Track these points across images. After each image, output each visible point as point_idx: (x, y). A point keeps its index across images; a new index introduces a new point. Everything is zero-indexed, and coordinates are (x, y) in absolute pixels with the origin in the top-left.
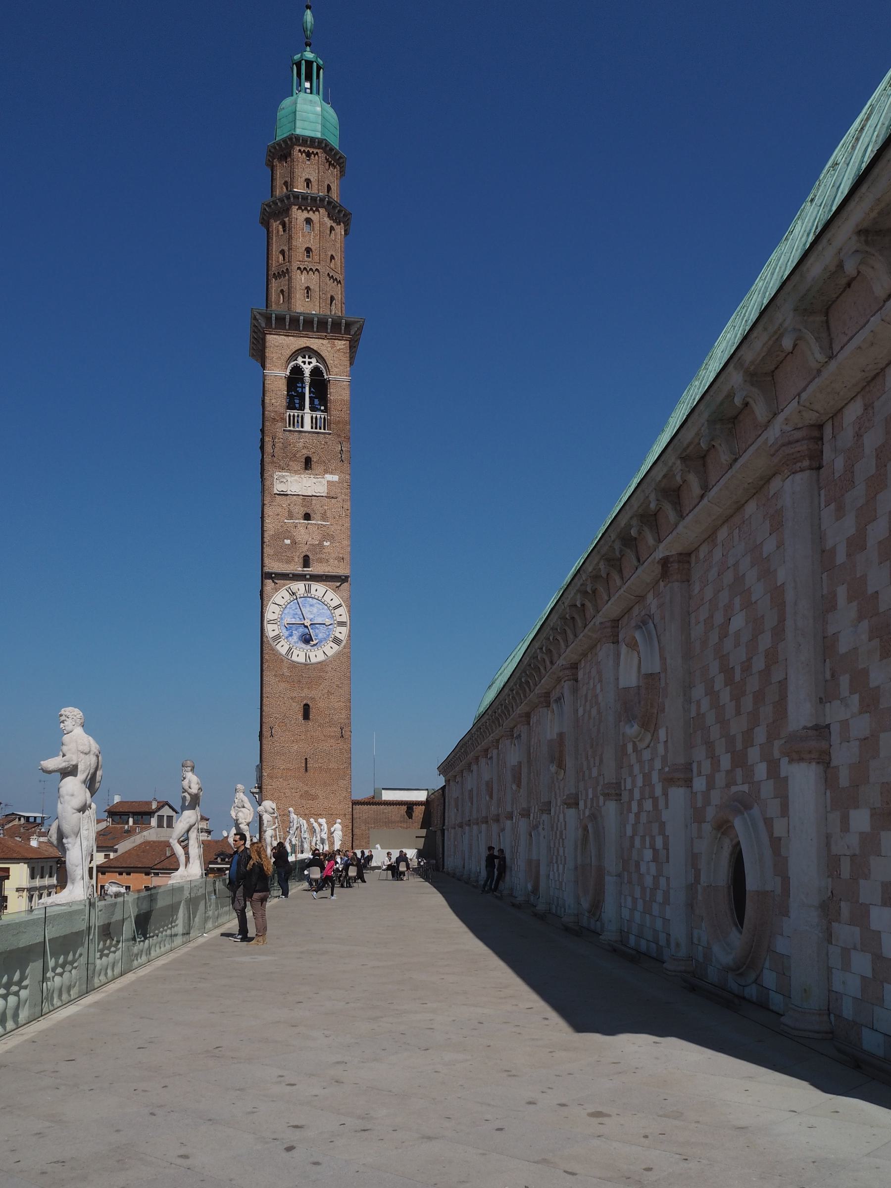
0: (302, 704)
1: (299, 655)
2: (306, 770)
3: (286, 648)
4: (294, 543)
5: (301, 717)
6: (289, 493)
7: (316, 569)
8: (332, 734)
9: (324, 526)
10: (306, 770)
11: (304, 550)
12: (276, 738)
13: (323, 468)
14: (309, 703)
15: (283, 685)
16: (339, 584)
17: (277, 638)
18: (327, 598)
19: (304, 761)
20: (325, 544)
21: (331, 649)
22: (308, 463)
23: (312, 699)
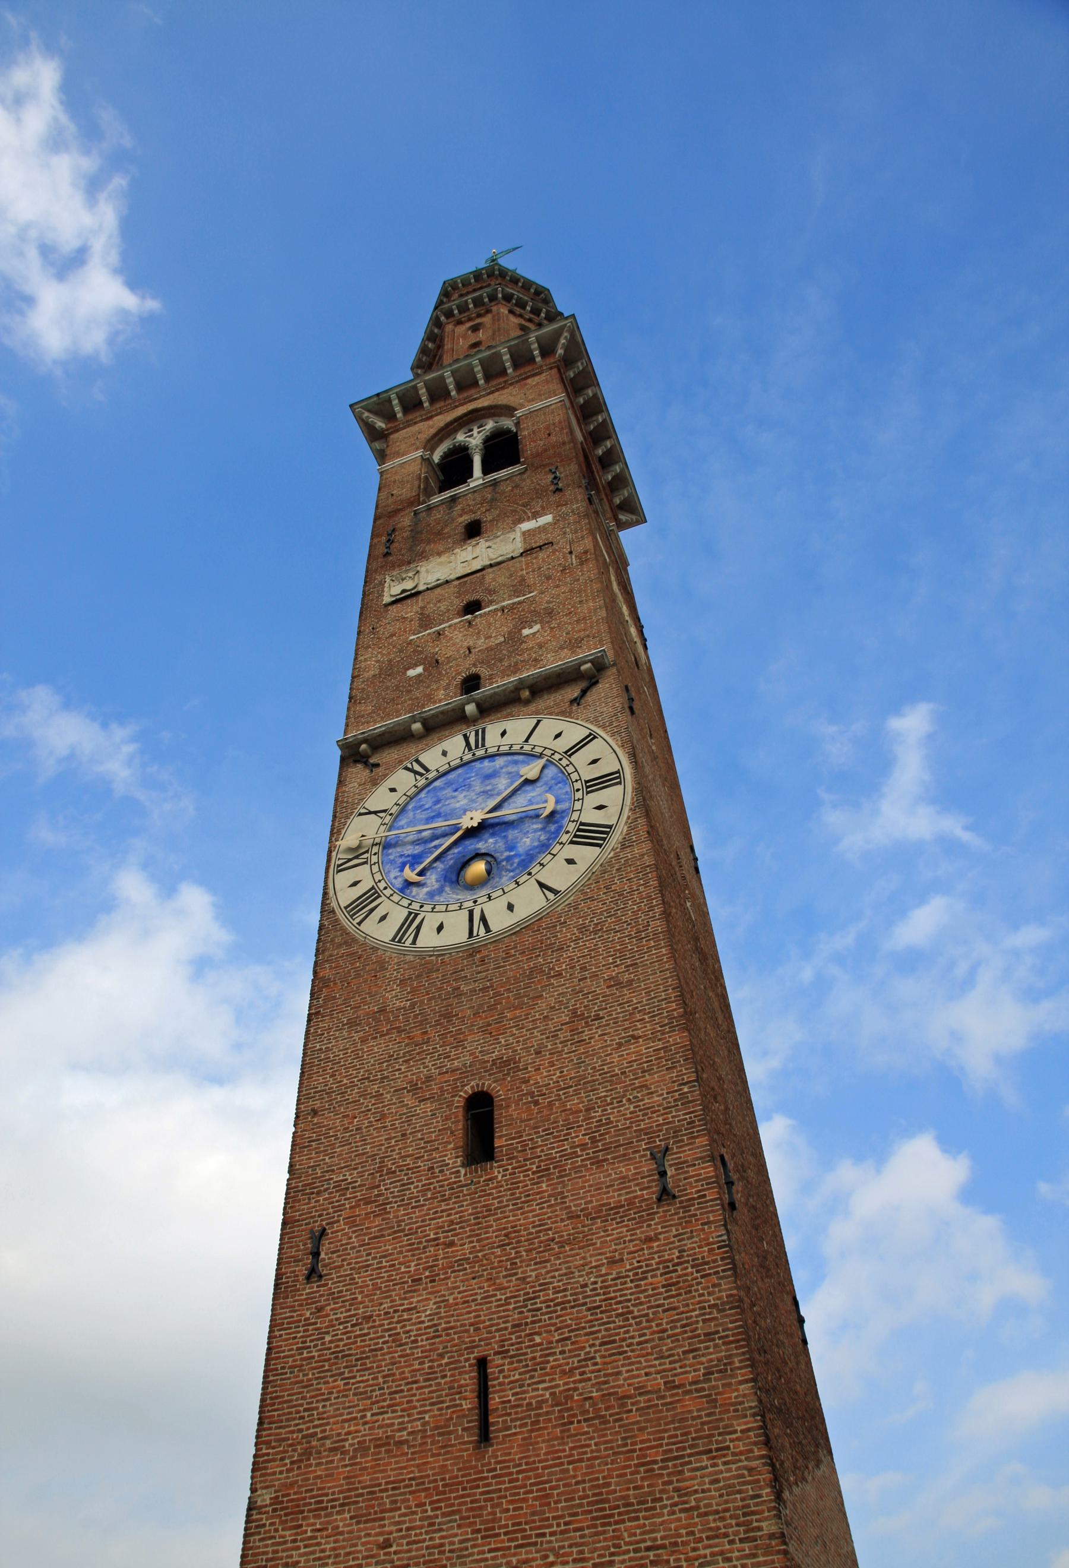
0: (459, 1101)
1: (446, 929)
2: (484, 1435)
3: (398, 915)
4: (434, 664)
5: (453, 1159)
6: (421, 588)
7: (493, 686)
8: (614, 1197)
9: (520, 603)
10: (484, 1435)
11: (466, 668)
12: (333, 1282)
13: (510, 520)
14: (489, 1084)
15: (378, 1047)
16: (576, 693)
17: (368, 900)
18: (543, 738)
19: (468, 1379)
20: (526, 632)
21: (566, 868)
22: (473, 531)
23: (506, 1065)
